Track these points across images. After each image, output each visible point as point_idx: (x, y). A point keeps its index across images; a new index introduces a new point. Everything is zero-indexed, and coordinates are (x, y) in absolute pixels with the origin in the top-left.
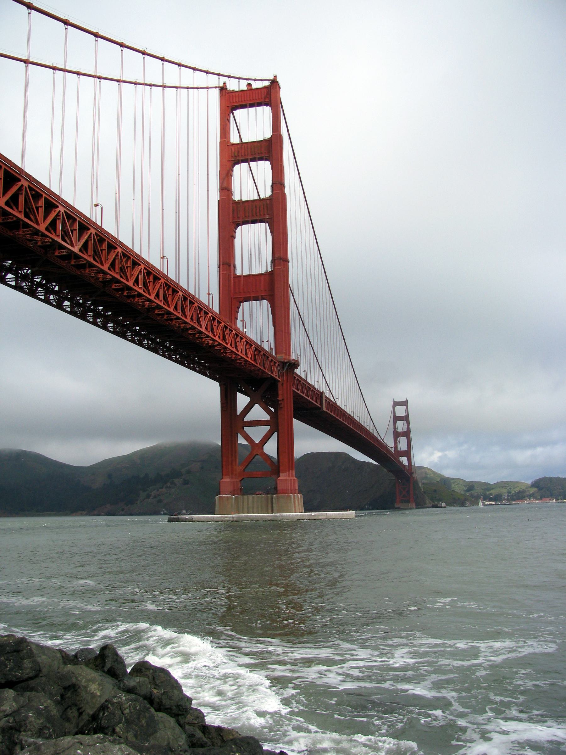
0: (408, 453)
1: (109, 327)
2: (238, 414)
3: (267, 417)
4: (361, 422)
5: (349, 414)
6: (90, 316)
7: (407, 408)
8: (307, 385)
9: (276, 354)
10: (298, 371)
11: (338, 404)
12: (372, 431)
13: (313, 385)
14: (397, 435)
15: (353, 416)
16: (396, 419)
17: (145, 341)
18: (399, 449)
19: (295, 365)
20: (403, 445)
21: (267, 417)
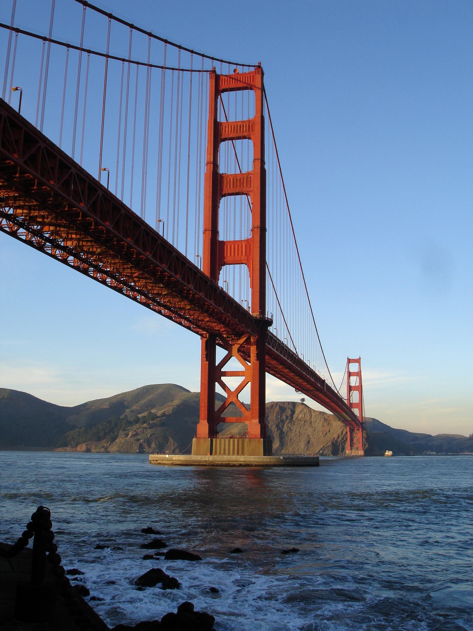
0: (360, 405)
1: (108, 282)
4: (321, 377)
5: (311, 369)
6: (91, 271)
8: (278, 341)
9: (253, 312)
12: (329, 385)
13: (282, 342)
14: (350, 388)
16: (350, 374)
17: (138, 296)
19: (270, 323)
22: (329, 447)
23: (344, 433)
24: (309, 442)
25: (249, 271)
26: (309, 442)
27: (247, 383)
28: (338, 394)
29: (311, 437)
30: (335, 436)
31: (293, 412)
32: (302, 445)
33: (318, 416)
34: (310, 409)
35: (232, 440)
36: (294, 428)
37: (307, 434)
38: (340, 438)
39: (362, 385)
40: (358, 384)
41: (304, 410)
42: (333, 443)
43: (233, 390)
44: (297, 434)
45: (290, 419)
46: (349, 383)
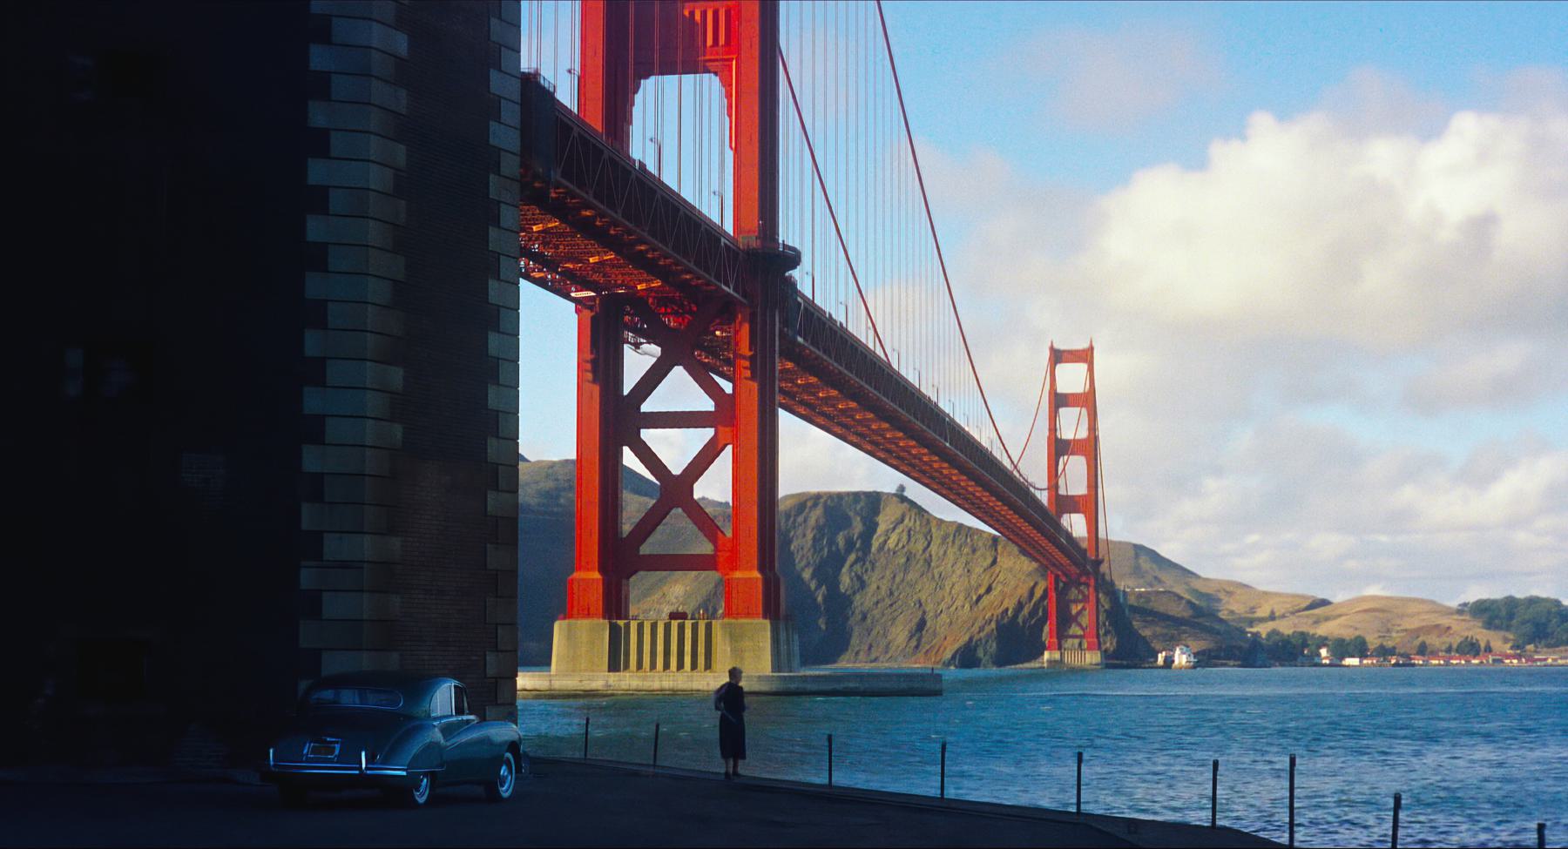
0: (1089, 505)
2: (626, 392)
3: (707, 404)
7: (1091, 370)
10: (795, 274)
11: (895, 366)
12: (985, 443)
13: (830, 315)
14: (1059, 448)
15: (934, 399)
16: (1059, 401)
18: (1062, 492)
19: (792, 258)
20: (1074, 478)
21: (707, 404)
22: (987, 641)
23: (1038, 593)
24: (921, 625)
25: (727, 97)
26: (921, 625)
27: (722, 449)
28: (1015, 473)
29: (930, 607)
30: (1010, 604)
31: (871, 528)
32: (900, 634)
33: (951, 538)
34: (925, 515)
35: (675, 623)
36: (873, 580)
37: (915, 597)
38: (1026, 611)
39: (1096, 439)
40: (1083, 434)
41: (906, 521)
42: (999, 627)
43: (676, 468)
44: (884, 600)
45: (858, 550)
46: (1053, 429)
